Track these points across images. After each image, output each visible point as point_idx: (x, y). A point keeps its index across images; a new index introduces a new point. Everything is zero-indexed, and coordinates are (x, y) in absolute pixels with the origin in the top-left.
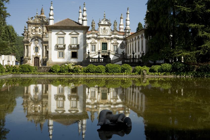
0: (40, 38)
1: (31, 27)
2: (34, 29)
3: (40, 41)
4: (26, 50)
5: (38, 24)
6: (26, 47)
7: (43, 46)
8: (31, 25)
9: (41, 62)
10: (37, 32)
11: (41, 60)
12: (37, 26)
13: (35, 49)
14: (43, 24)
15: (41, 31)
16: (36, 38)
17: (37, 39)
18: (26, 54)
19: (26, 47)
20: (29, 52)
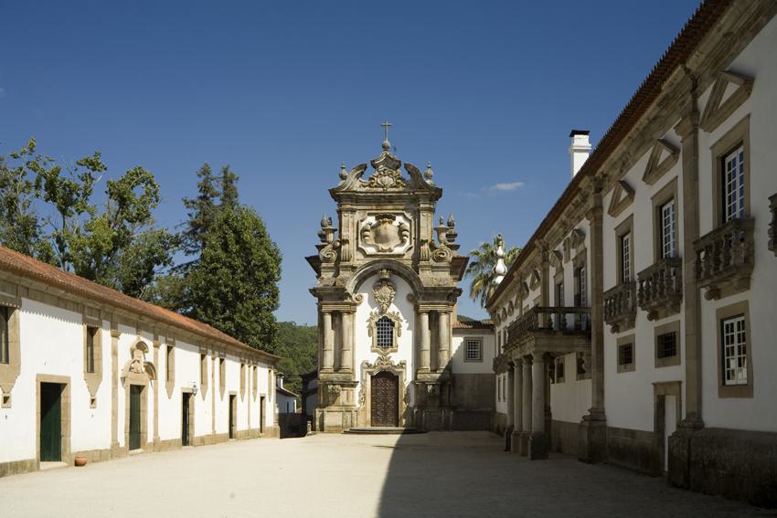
0: (399, 274)
1: (358, 216)
2: (369, 227)
3: (405, 289)
4: (330, 334)
5: (390, 200)
6: (328, 318)
7: (418, 314)
8: (355, 207)
9: (407, 399)
10: (385, 239)
11: (408, 389)
12: (389, 209)
13: (375, 331)
14: (415, 200)
15: (408, 234)
16: (384, 272)
17: (386, 280)
18: (329, 360)
19: (333, 321)
20: (346, 346)
